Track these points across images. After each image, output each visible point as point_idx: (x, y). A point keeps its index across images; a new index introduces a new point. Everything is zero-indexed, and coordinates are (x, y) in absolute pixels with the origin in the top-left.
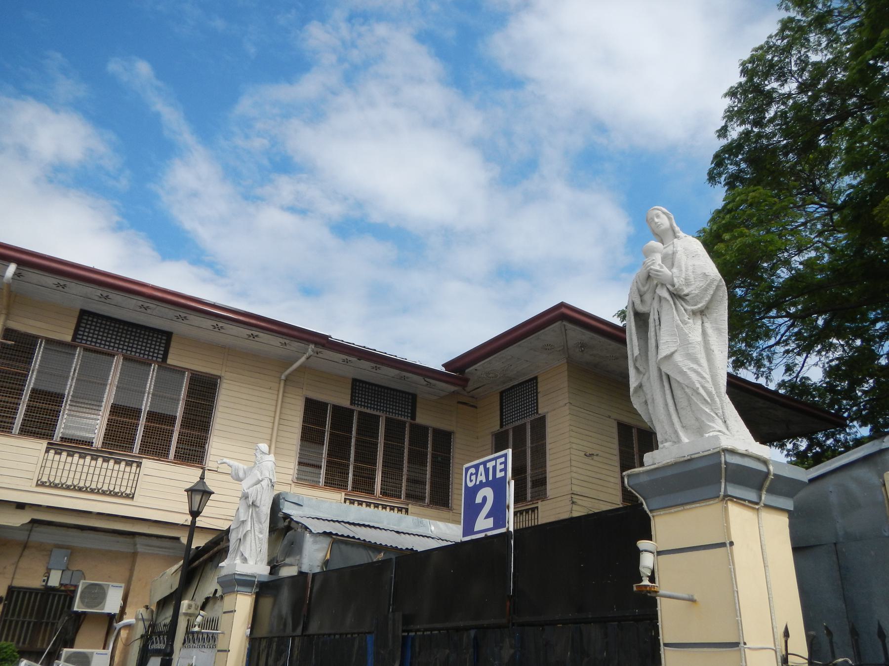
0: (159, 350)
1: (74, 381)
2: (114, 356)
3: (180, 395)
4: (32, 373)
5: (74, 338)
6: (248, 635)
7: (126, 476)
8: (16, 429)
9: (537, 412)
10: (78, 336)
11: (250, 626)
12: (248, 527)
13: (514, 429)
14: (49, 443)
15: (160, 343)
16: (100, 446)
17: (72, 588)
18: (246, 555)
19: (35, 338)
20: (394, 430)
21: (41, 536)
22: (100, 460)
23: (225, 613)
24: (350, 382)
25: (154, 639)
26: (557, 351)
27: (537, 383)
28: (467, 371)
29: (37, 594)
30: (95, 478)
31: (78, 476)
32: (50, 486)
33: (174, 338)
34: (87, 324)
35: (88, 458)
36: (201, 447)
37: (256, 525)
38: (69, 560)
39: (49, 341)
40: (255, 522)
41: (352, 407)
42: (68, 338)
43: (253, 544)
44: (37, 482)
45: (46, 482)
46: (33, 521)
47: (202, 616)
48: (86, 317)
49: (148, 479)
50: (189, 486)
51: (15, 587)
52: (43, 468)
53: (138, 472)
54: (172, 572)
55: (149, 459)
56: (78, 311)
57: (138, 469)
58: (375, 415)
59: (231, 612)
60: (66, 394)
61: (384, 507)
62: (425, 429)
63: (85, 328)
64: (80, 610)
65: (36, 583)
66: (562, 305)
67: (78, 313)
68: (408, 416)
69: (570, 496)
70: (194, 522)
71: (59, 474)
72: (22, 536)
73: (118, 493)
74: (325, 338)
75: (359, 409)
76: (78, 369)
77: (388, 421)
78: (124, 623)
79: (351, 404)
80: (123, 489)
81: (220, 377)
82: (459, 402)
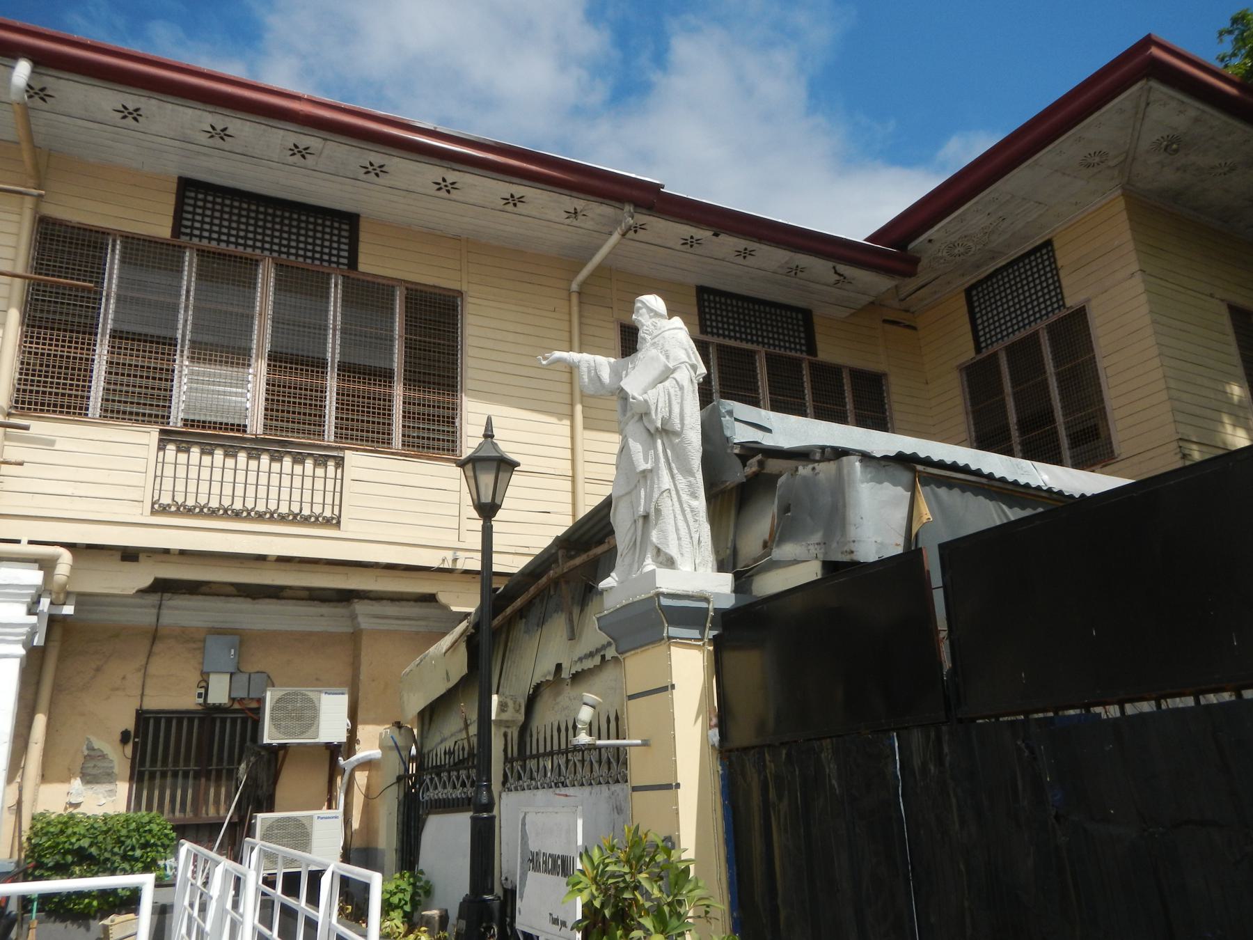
0: (339, 249)
1: (190, 313)
2: (256, 263)
3: (392, 331)
4: (107, 300)
5: (177, 230)
6: (717, 744)
7: (319, 484)
8: (94, 408)
9: (1064, 305)
10: (183, 230)
11: (715, 721)
12: (666, 481)
13: (1010, 350)
14: (162, 432)
15: (340, 236)
16: (260, 431)
17: (254, 705)
18: (673, 550)
19: (104, 233)
23: (631, 697)
24: (694, 292)
25: (428, 780)
26: (1109, 167)
27: (1053, 251)
28: (911, 246)
29: (191, 721)
31: (228, 490)
32: (178, 513)
33: (363, 226)
34: (195, 206)
36: (448, 422)
37: (679, 477)
38: (239, 655)
40: (675, 471)
42: (164, 230)
43: (681, 524)
44: (153, 507)
45: (169, 505)
46: (161, 587)
47: (593, 707)
48: (193, 195)
52: (158, 480)
53: (339, 476)
54: (444, 651)
55: (357, 450)
56: (176, 180)
57: (339, 471)
58: (747, 350)
59: (665, 689)
60: (179, 336)
64: (275, 742)
65: (189, 702)
67: (175, 186)
69: (1175, 445)
71: (192, 488)
72: (144, 616)
73: (310, 517)
74: (655, 189)
76: (192, 289)
77: (770, 358)
78: (358, 759)
80: (317, 510)
81: (460, 293)
82: (885, 321)
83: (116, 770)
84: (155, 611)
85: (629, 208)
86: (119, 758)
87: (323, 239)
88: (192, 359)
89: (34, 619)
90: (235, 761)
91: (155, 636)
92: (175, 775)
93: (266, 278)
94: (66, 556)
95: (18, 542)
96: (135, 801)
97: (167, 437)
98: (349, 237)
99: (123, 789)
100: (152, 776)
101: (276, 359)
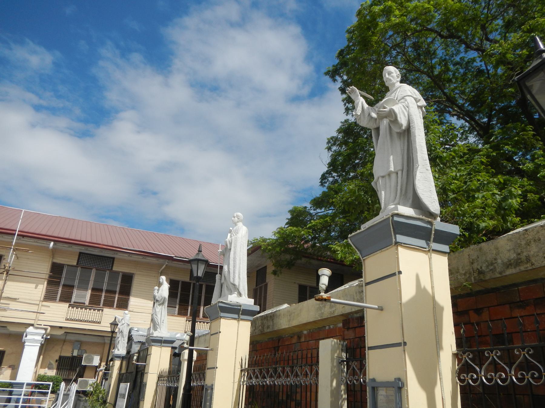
5: (77, 264)
12: (120, 339)
14: (69, 304)
18: (119, 348)
19: (64, 265)
27: (266, 269)
31: (80, 316)
33: (115, 260)
38: (80, 346)
39: (68, 265)
41: (191, 282)
50: (111, 322)
61: (204, 322)
63: (82, 259)
64: (84, 364)
65: (69, 354)
70: (112, 335)
71: (73, 315)
72: (63, 338)
77: (206, 285)
79: (190, 280)
80: (97, 320)
81: (133, 274)
83: (54, 367)
85: (167, 261)
86: (55, 365)
87: (107, 263)
88: (77, 290)
89: (42, 339)
90: (77, 367)
91: (65, 341)
92: (65, 369)
93: (94, 272)
94: (49, 328)
95: (41, 325)
96: (57, 373)
99: (55, 371)
100: (61, 369)
101: (93, 289)
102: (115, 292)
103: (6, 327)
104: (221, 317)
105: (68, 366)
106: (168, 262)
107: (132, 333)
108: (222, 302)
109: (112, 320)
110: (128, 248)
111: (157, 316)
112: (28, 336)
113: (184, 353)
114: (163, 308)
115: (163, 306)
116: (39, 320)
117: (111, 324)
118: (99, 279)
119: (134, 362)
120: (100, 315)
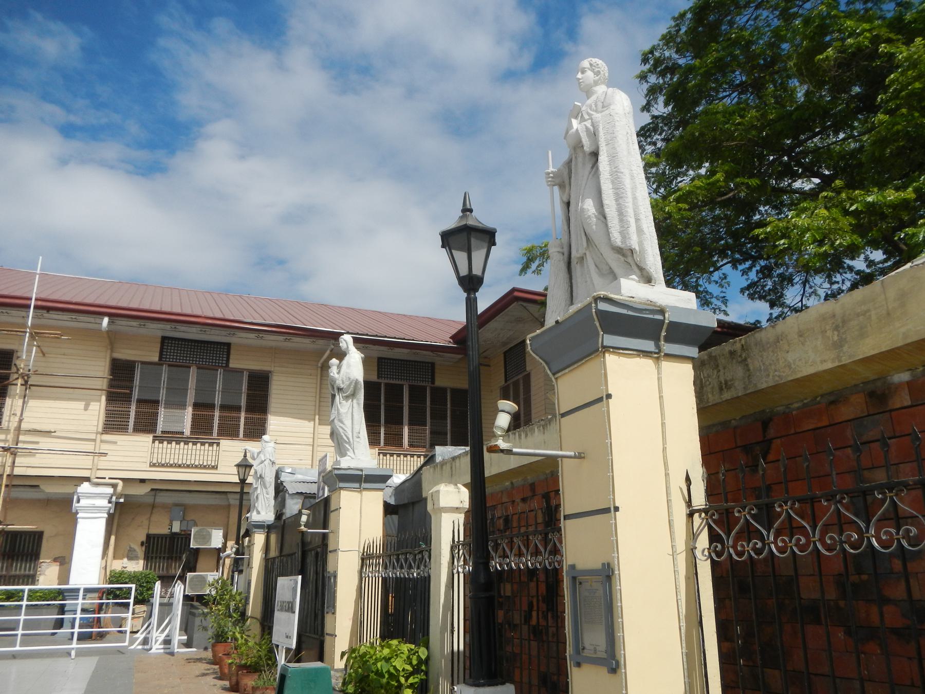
0: (223, 357)
2: (190, 367)
5: (161, 358)
7: (210, 453)
12: (259, 491)
13: (513, 382)
14: (154, 436)
18: (259, 509)
19: (134, 362)
20: (417, 394)
21: (162, 499)
22: (190, 444)
29: (166, 538)
30: (189, 457)
31: (176, 457)
32: (159, 466)
33: (232, 346)
34: (168, 346)
35: (182, 444)
38: (184, 513)
39: (143, 363)
41: (380, 381)
43: (263, 502)
48: (167, 341)
49: (227, 453)
51: (150, 534)
61: (412, 456)
62: (443, 390)
63: (167, 349)
64: (195, 547)
65: (165, 531)
66: (514, 290)
68: (428, 381)
71: (164, 457)
72: (150, 500)
75: (386, 381)
77: (412, 388)
79: (378, 377)
80: (209, 463)
81: (270, 372)
83: (139, 555)
84: (153, 497)
86: (140, 551)
88: (165, 408)
89: (110, 505)
90: (181, 553)
91: (153, 506)
92: (160, 558)
93: (193, 371)
94: (120, 483)
95: (105, 478)
96: (146, 567)
97: (155, 438)
98: (227, 352)
99: (141, 562)
100: (152, 558)
101: (196, 406)
102: (238, 409)
103: (37, 486)
104: (606, 349)
105: (165, 553)
106: (333, 345)
107: (282, 479)
108: (607, 300)
109: (239, 459)
110: (254, 321)
111: (342, 422)
112: (81, 501)
113: (438, 492)
114: (355, 405)
115: (355, 401)
116: (98, 469)
117: (238, 466)
118: (205, 388)
119: (303, 527)
120: (214, 453)
